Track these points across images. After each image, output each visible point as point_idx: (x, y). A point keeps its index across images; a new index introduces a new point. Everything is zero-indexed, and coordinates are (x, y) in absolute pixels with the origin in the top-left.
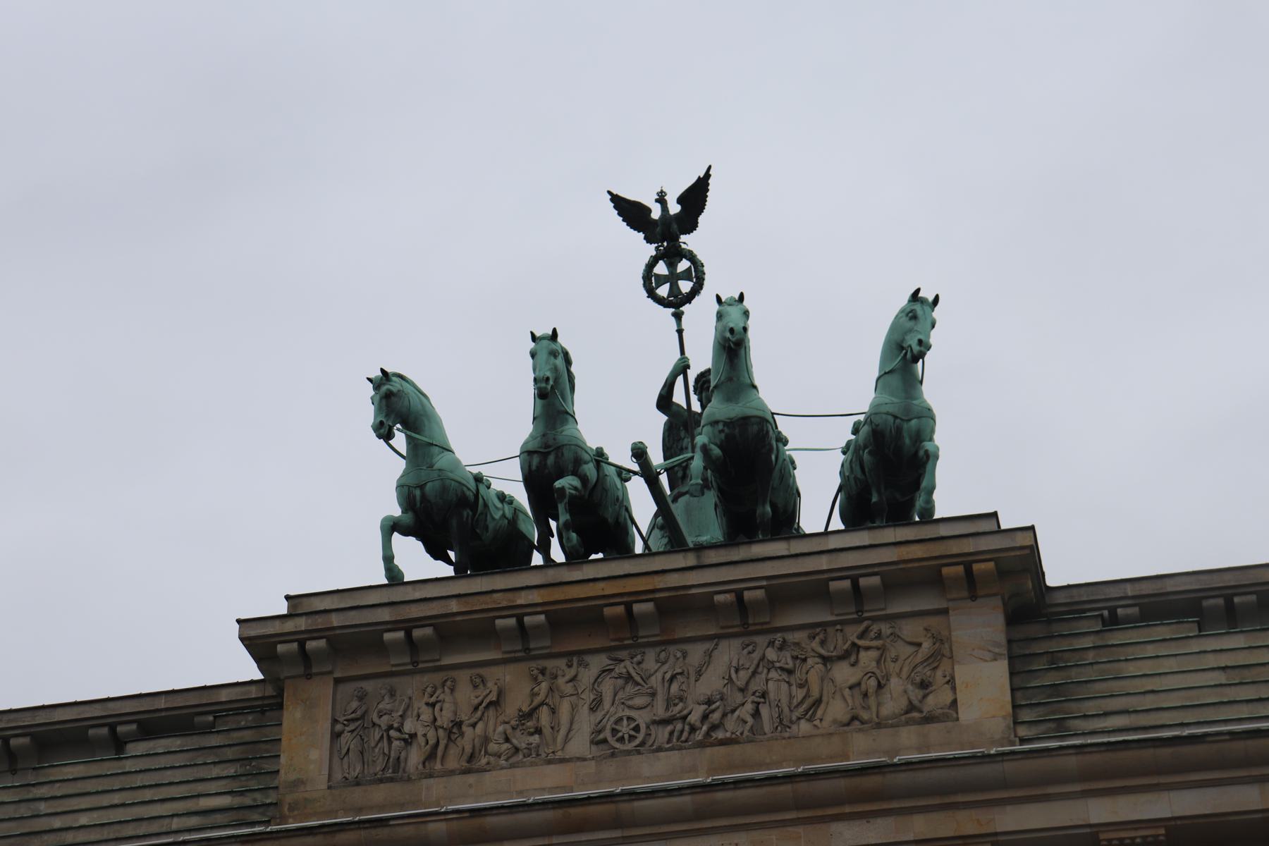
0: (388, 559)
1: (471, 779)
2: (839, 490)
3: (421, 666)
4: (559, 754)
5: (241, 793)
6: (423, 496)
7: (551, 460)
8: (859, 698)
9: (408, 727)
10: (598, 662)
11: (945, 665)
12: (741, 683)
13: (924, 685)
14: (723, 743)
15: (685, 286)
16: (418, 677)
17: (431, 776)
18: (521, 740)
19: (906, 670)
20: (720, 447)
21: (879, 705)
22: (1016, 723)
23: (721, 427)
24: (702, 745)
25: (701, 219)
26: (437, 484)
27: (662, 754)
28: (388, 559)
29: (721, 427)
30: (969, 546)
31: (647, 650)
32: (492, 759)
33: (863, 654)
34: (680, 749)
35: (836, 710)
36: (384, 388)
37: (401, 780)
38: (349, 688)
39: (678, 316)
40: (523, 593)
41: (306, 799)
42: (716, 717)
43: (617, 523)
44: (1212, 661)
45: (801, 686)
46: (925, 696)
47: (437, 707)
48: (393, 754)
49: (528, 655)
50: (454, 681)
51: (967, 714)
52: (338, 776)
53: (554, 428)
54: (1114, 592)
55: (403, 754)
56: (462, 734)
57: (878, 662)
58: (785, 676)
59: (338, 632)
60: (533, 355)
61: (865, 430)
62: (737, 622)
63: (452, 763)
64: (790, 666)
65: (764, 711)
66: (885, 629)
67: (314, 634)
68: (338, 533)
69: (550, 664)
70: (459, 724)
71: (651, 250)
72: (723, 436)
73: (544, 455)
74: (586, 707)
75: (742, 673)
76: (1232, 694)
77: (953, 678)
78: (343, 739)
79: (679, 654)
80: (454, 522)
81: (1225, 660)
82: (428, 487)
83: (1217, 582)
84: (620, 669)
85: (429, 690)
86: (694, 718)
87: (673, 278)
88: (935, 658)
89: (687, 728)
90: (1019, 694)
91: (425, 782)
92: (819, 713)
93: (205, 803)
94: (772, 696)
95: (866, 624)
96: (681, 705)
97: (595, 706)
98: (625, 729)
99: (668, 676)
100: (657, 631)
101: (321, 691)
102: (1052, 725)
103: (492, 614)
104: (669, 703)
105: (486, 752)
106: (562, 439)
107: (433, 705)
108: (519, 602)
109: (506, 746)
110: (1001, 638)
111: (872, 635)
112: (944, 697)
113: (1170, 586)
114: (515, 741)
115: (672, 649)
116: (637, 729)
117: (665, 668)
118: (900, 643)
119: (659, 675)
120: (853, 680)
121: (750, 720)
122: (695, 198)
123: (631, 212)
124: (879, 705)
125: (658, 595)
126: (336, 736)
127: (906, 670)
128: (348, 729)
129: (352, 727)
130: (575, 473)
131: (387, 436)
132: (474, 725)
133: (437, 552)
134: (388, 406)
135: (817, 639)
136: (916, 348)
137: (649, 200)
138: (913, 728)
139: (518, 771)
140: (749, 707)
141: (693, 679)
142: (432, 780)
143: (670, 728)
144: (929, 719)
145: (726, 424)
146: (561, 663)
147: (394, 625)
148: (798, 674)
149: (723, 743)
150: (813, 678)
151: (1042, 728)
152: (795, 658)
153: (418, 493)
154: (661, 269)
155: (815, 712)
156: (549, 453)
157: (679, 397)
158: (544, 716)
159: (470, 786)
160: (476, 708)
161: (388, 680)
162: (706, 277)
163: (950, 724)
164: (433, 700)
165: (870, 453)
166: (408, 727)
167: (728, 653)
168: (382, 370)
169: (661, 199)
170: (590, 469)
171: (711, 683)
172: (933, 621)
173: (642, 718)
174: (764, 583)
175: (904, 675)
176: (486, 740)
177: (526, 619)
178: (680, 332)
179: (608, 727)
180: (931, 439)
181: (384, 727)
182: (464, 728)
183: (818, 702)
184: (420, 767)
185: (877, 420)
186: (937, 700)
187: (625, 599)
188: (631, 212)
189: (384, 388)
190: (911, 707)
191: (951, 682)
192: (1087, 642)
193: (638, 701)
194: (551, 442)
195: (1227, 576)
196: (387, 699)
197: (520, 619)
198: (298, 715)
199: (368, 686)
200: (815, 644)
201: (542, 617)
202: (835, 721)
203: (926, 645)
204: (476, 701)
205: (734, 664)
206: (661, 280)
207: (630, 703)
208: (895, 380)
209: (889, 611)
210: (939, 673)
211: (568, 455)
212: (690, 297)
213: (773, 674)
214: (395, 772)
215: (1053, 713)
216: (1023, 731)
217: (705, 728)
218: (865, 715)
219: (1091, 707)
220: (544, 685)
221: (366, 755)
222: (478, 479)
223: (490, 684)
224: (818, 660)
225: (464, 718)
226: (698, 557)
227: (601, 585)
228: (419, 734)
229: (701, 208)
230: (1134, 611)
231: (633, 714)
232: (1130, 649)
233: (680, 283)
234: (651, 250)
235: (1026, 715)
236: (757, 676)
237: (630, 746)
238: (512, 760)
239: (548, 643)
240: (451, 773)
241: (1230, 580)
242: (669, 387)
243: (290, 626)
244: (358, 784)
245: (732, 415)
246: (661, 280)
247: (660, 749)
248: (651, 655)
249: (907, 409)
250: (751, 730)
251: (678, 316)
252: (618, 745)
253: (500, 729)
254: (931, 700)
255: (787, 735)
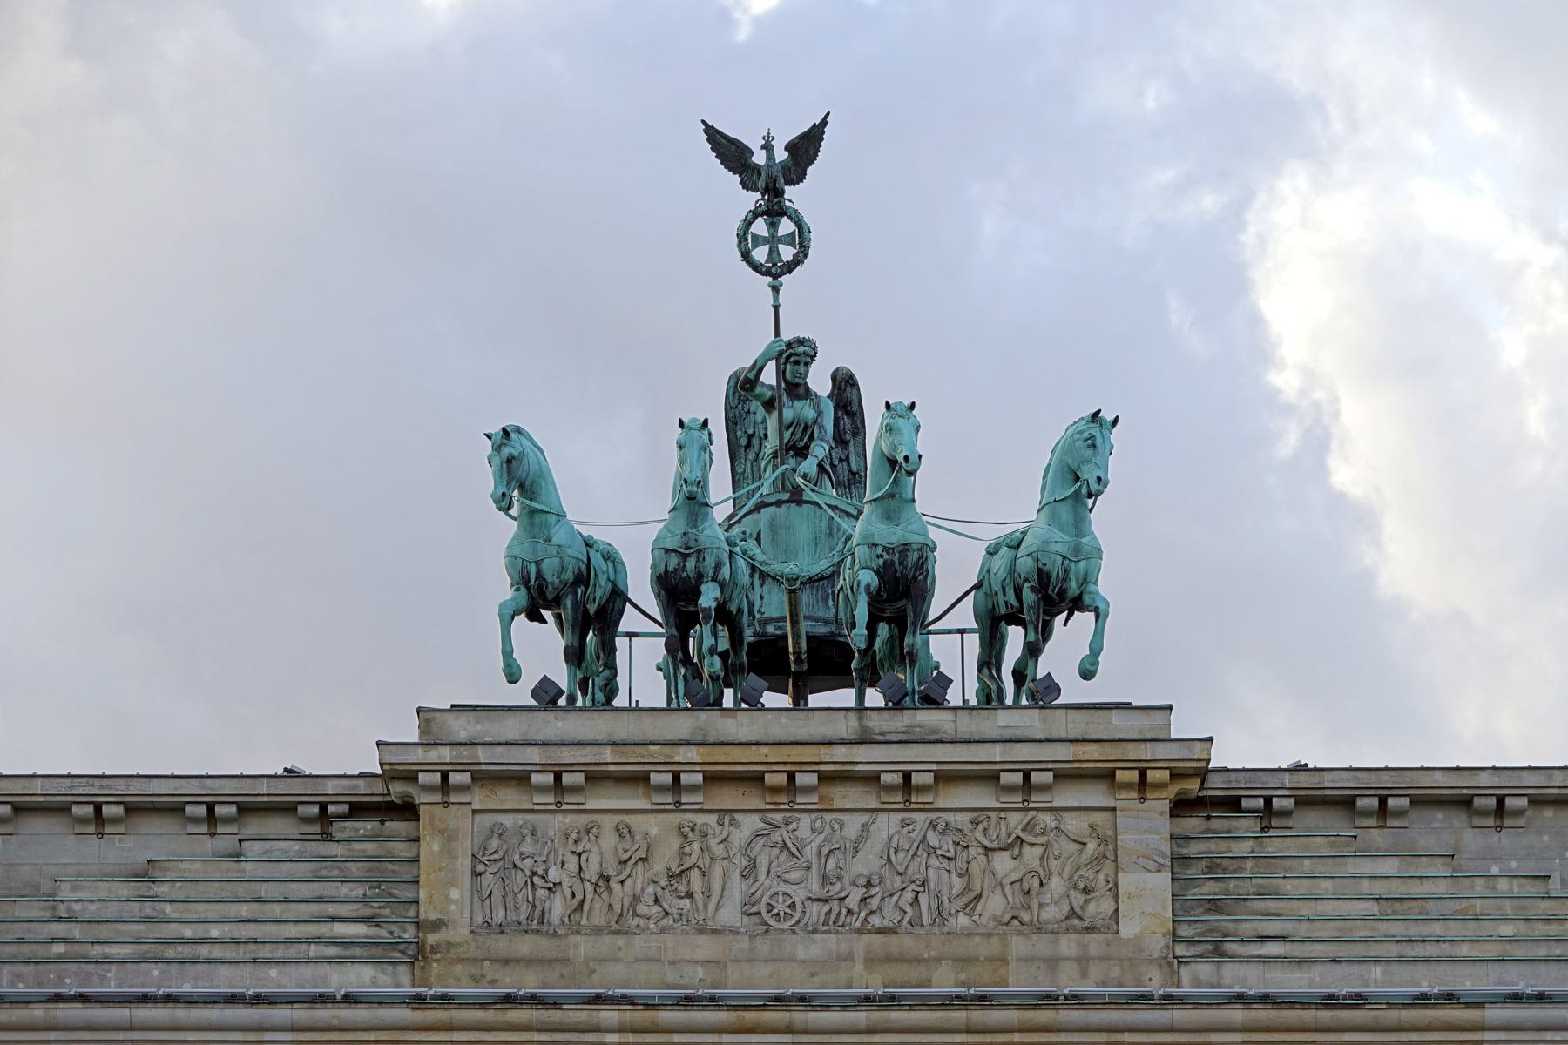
0: (507, 654)
1: (620, 941)
2: (978, 586)
3: (565, 807)
4: (711, 925)
5: (378, 925)
6: (539, 572)
7: (691, 564)
8: (1019, 899)
9: (554, 875)
10: (751, 823)
11: (1108, 868)
12: (901, 869)
13: (1086, 891)
14: (880, 931)
15: (787, 253)
16: (559, 817)
17: (578, 933)
18: (670, 902)
19: (1067, 869)
20: (877, 573)
21: (1041, 905)
22: (1174, 934)
23: (879, 551)
24: (860, 932)
25: (809, 170)
26: (556, 562)
27: (817, 937)
28: (507, 654)
29: (879, 551)
30: (1146, 752)
31: (802, 816)
32: (642, 922)
33: (1026, 849)
34: (837, 933)
35: (994, 905)
36: (506, 451)
37: (547, 933)
38: (489, 819)
39: (776, 289)
40: (682, 749)
41: (449, 943)
42: (875, 902)
43: (740, 610)
44: (1365, 887)
45: (960, 876)
46: (1087, 902)
47: (583, 857)
48: (539, 908)
49: (678, 808)
50: (599, 827)
51: (1129, 928)
52: (479, 919)
53: (695, 526)
54: (1272, 781)
55: (547, 905)
56: (609, 888)
57: (1042, 858)
58: (945, 863)
59: (484, 767)
60: (680, 448)
61: (1025, 565)
62: (899, 798)
63: (599, 918)
64: (951, 855)
65: (923, 898)
66: (1048, 819)
67: (460, 767)
68: (479, 655)
69: (700, 819)
70: (607, 879)
71: (752, 199)
72: (881, 561)
73: (685, 557)
74: (737, 873)
75: (901, 855)
76: (1384, 928)
77: (1116, 885)
78: (488, 879)
79: (836, 826)
80: (569, 602)
81: (1380, 888)
82: (544, 566)
83: (1373, 781)
84: (776, 837)
85: (574, 835)
86: (852, 902)
87: (773, 241)
88: (1098, 859)
89: (844, 911)
90: (1178, 905)
91: (573, 939)
92: (979, 908)
93: (340, 929)
94: (932, 885)
95: (1032, 813)
96: (838, 886)
97: (749, 872)
98: (781, 908)
99: (825, 851)
100: (815, 800)
101: (457, 818)
102: (1210, 947)
103: (647, 768)
104: (825, 879)
105: (636, 914)
106: (704, 541)
107: (580, 854)
108: (677, 759)
109: (656, 909)
110: (1166, 847)
111: (1038, 830)
112: (1107, 906)
113: (1328, 781)
114: (666, 906)
115: (828, 817)
116: (793, 906)
117: (822, 837)
118: (1063, 837)
119: (814, 845)
120: (1015, 877)
121: (908, 909)
122: (806, 147)
123: (730, 152)
124: (1041, 905)
125: (822, 768)
126: (476, 874)
127: (1067, 869)
128: (490, 870)
129: (494, 868)
130: (714, 579)
131: (504, 503)
132: (622, 882)
133: (534, 616)
134: (509, 472)
135: (981, 827)
136: (1094, 487)
137: (754, 144)
138: (1073, 936)
139: (669, 939)
140: (909, 895)
141: (849, 856)
142: (579, 938)
143: (826, 908)
144: (1090, 929)
145: (885, 549)
146: (712, 819)
147: (543, 768)
148: (959, 864)
149: (880, 931)
150: (975, 868)
151: (1200, 949)
152: (957, 844)
153: (533, 568)
154: (760, 227)
155: (973, 909)
156: (689, 555)
157: (769, 376)
158: (696, 883)
159: (620, 949)
160: (626, 862)
161: (528, 817)
162: (812, 244)
163: (1110, 936)
164: (579, 849)
165: (1032, 589)
166: (554, 875)
167: (887, 824)
168: (504, 430)
169: (768, 147)
170: (725, 572)
171: (867, 862)
172: (1099, 818)
173: (799, 894)
174: (934, 767)
175: (1066, 876)
176: (636, 899)
177: (683, 776)
178: (776, 308)
179: (765, 899)
180: (1096, 583)
181: (528, 873)
182: (615, 885)
183: (980, 896)
184: (566, 920)
185: (1044, 559)
186: (1100, 907)
187: (788, 768)
188: (730, 152)
189: (506, 451)
190: (1073, 913)
191: (1114, 889)
192: (1242, 848)
193: (794, 875)
194: (692, 544)
195: (1385, 777)
196: (528, 839)
197: (676, 777)
198: (436, 848)
199: (508, 821)
200: (979, 834)
201: (700, 777)
202: (995, 918)
203: (1091, 846)
204: (625, 856)
205: (894, 844)
206: (757, 241)
207: (786, 876)
208: (1065, 512)
209: (1055, 805)
210: (1101, 876)
211: (710, 561)
212: (790, 267)
213: (933, 861)
214: (539, 922)
215: (1211, 931)
216: (1180, 950)
217: (863, 914)
218: (1026, 917)
219: (1247, 929)
220: (696, 846)
221: (508, 899)
222: (588, 544)
223: (638, 838)
224: (981, 850)
225: (612, 873)
226: (860, 719)
227: (765, 749)
228: (565, 885)
229: (812, 160)
230: (1289, 803)
231: (789, 889)
232: (1288, 863)
233: (781, 247)
234: (752, 199)
235: (1185, 931)
236: (917, 859)
237: (786, 926)
238: (664, 923)
239: (700, 799)
240: (597, 931)
241: (1387, 780)
242: (758, 368)
243: (433, 755)
244: (502, 932)
245: (893, 539)
246: (757, 241)
247: (815, 931)
248: (806, 820)
249: (1077, 550)
250: (910, 923)
251: (776, 289)
252: (772, 922)
253: (651, 889)
254: (1092, 908)
255: (946, 930)
